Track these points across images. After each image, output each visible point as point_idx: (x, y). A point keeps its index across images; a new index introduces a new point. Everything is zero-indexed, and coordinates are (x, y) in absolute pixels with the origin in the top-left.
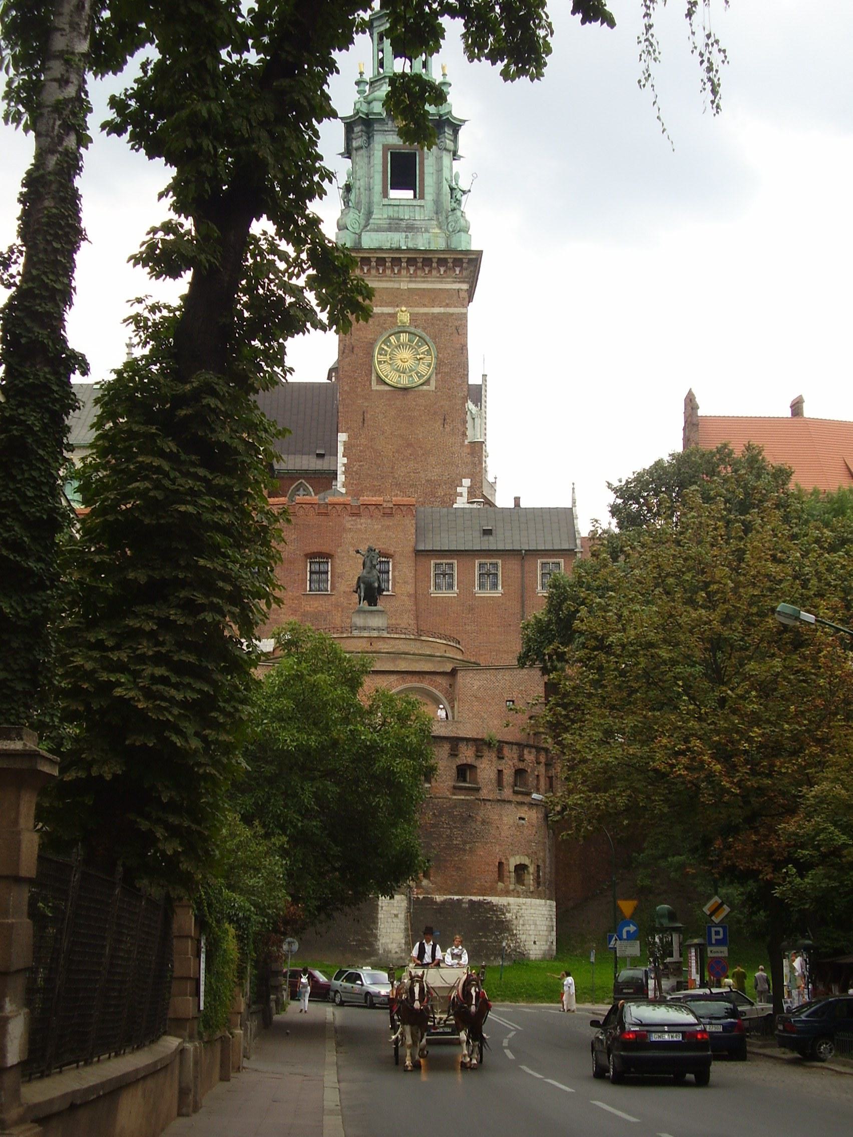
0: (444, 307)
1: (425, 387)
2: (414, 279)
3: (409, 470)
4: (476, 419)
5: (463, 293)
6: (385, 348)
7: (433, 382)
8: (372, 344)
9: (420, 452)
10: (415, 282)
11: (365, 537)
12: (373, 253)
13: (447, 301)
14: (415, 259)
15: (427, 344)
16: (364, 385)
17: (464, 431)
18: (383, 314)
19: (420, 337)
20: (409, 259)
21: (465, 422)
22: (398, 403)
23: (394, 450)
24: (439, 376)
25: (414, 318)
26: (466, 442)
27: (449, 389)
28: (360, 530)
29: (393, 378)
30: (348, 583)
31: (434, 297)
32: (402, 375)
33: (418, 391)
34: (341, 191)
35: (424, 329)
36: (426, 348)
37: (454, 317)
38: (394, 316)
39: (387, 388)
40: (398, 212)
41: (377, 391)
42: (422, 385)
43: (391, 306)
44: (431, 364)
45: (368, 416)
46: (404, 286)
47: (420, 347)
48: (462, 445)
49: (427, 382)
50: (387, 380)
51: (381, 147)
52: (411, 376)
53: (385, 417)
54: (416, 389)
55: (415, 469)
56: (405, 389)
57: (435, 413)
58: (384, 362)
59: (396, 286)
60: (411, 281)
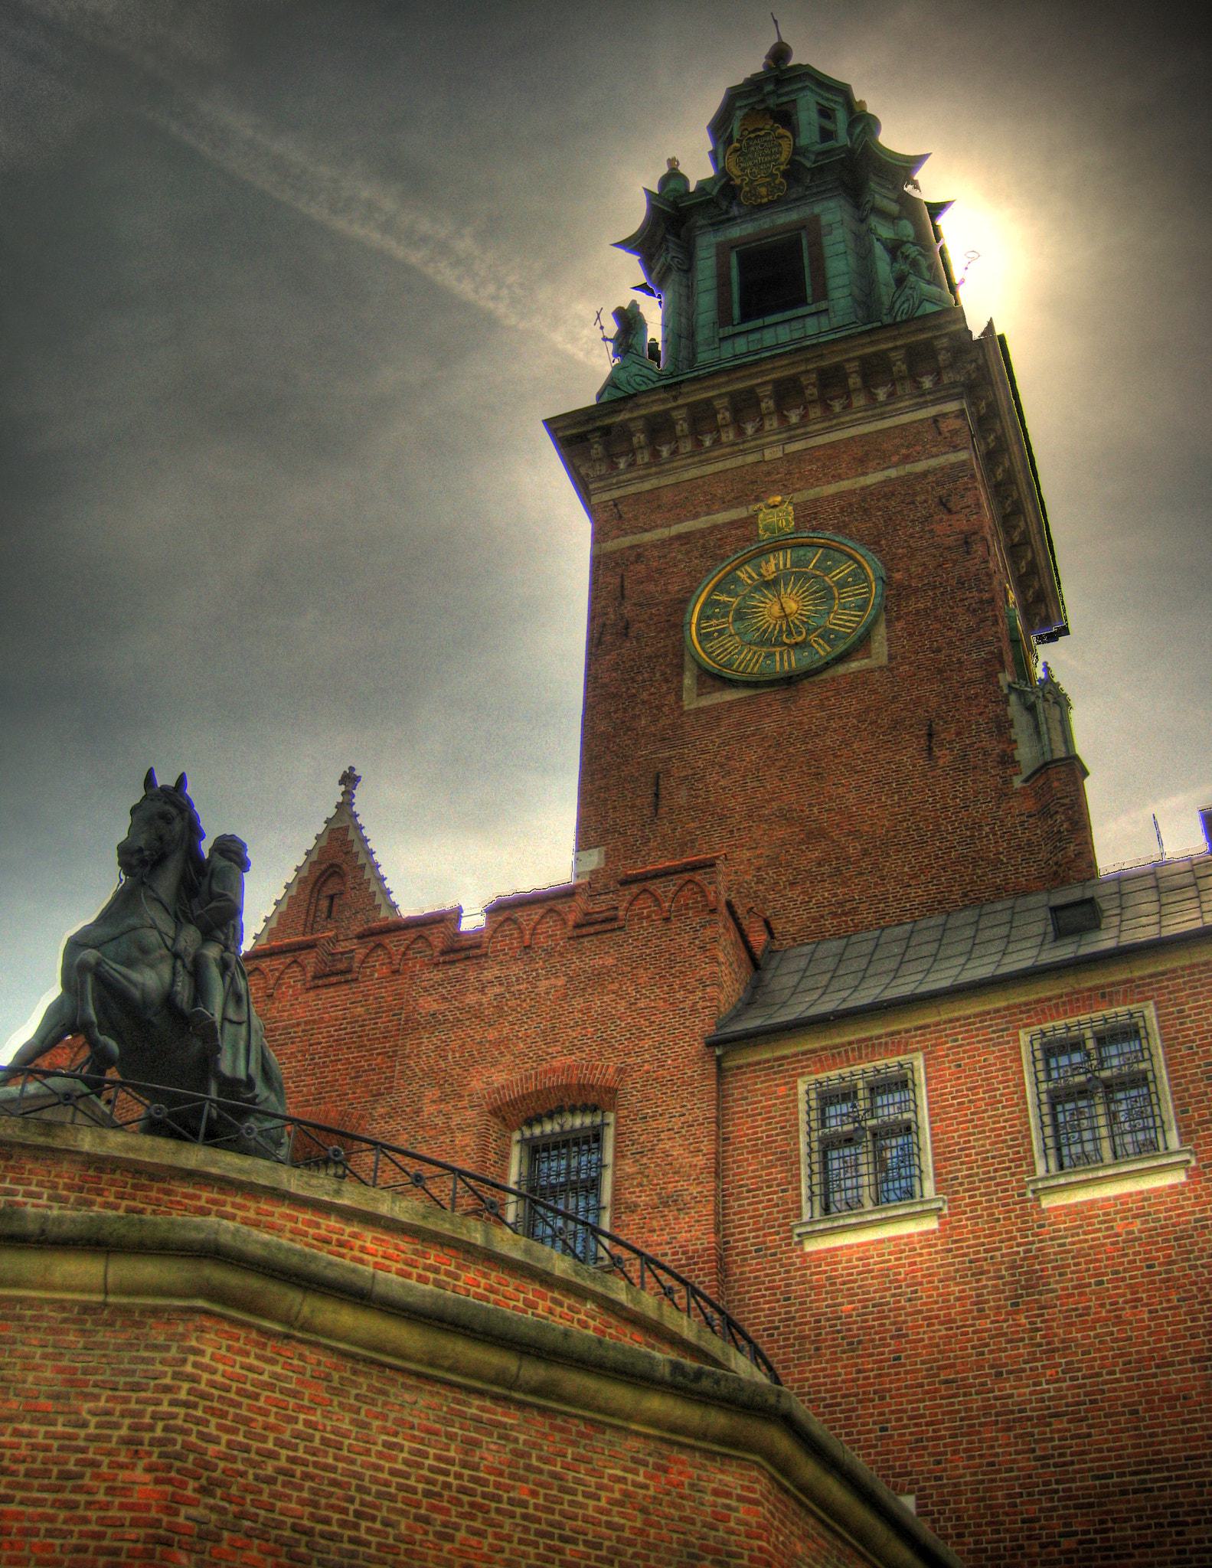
0: (895, 465)
1: (854, 665)
3: (814, 912)
4: (1040, 705)
5: (950, 421)
6: (723, 598)
7: (880, 647)
9: (853, 849)
10: (807, 436)
11: (492, 1034)
13: (904, 451)
14: (794, 379)
15: (851, 557)
16: (659, 708)
17: (1004, 751)
18: (715, 527)
20: (777, 383)
21: (1002, 727)
22: (769, 726)
23: (762, 862)
24: (900, 625)
25: (807, 515)
26: (1017, 783)
27: (939, 650)
28: (476, 1013)
31: (867, 453)
33: (833, 679)
34: (610, 346)
35: (840, 529)
37: (931, 478)
38: (752, 519)
39: (730, 695)
40: (761, 340)
43: (741, 504)
44: (866, 601)
46: (769, 454)
47: (830, 569)
48: (1004, 793)
50: (727, 673)
51: (713, 251)
54: (825, 676)
55: (840, 904)
56: (789, 681)
57: (896, 724)
58: (721, 632)
60: (791, 440)
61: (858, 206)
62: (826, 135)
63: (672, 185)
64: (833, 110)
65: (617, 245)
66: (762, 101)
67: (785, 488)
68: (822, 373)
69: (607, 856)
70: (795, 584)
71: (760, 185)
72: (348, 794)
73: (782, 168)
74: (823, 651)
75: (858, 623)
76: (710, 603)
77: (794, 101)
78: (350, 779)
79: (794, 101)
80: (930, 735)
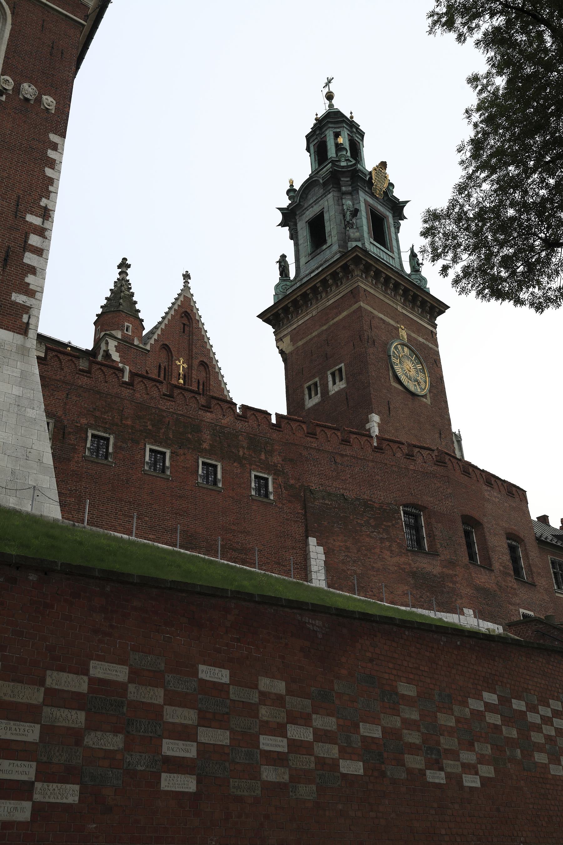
2: (405, 307)
8: (386, 344)
12: (385, 269)
15: (421, 364)
18: (389, 324)
19: (416, 356)
21: (453, 443)
24: (432, 394)
30: (500, 561)
38: (397, 329)
41: (395, 387)
42: (422, 396)
45: (391, 407)
46: (399, 309)
49: (424, 396)
53: (403, 414)
54: (419, 398)
56: (413, 394)
59: (395, 306)
60: (403, 308)
69: (381, 419)
71: (378, 190)
72: (186, 283)
73: (384, 189)
78: (187, 276)
80: (440, 434)
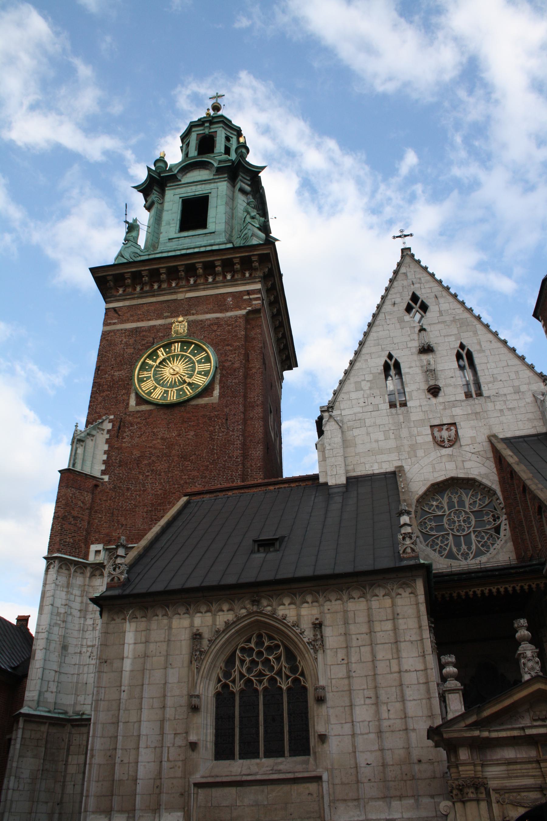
29: (157, 395)
32: (170, 390)
36: (203, 355)
46: (180, 296)
52: (182, 389)
61: (234, 186)
62: (227, 151)
63: (160, 164)
64: (232, 138)
65: (134, 187)
66: (204, 130)
67: (184, 315)
68: (204, 263)
70: (180, 360)
74: (189, 392)
75: (204, 382)
76: (144, 363)
77: (216, 132)
79: (216, 132)
